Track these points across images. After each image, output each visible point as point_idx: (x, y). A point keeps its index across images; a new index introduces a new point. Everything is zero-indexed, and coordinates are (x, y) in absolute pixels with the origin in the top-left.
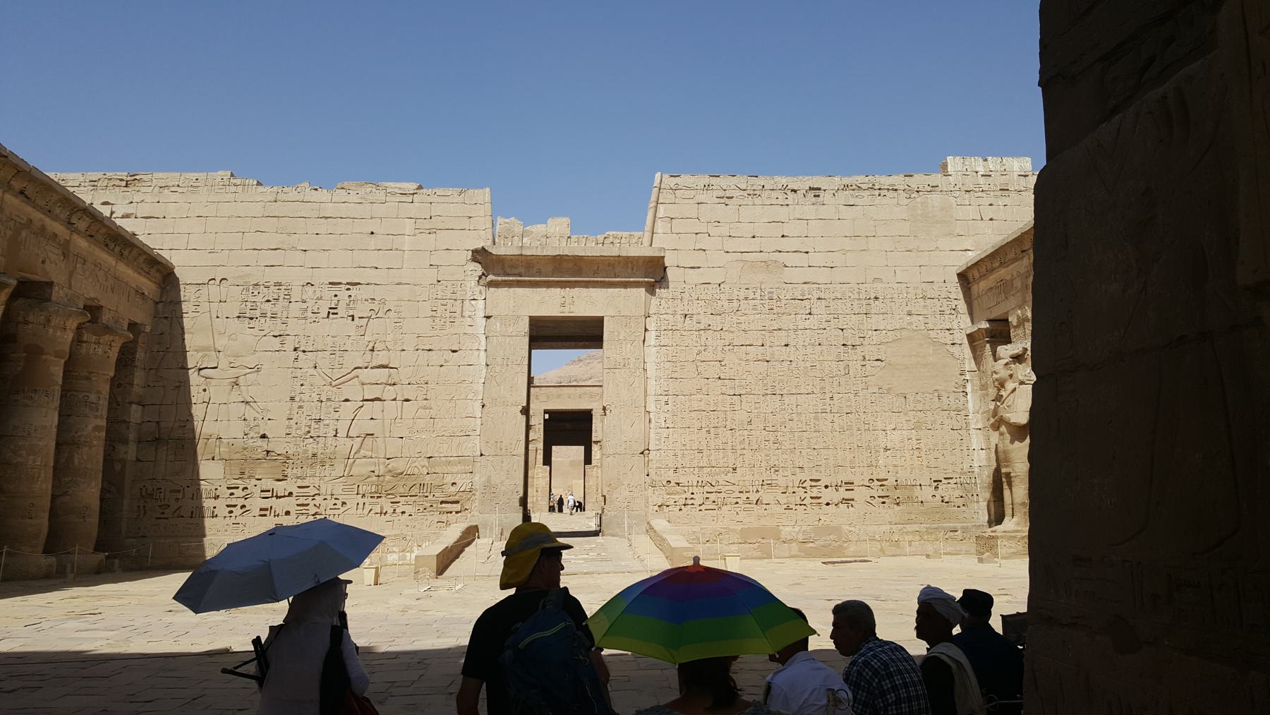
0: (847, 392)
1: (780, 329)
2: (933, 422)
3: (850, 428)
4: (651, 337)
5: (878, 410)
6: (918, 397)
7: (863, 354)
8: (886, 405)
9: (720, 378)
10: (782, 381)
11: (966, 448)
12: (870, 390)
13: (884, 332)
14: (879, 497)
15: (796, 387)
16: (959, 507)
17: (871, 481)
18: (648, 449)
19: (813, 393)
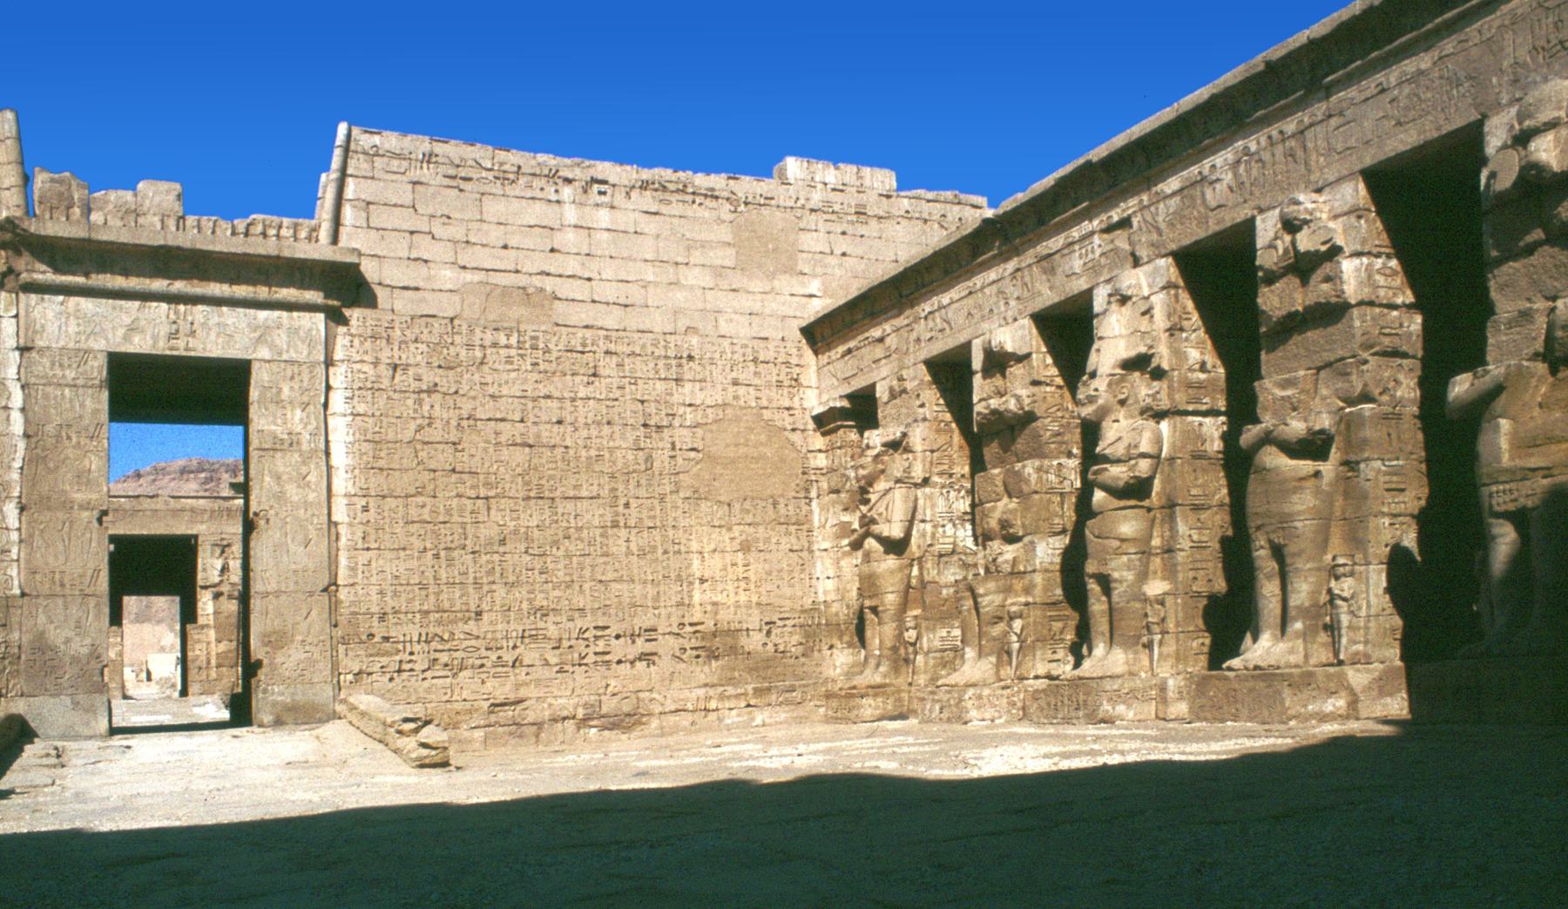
2: (767, 541)
4: (338, 401)
6: (747, 505)
9: (453, 470)
12: (682, 495)
18: (335, 584)
19: (598, 497)
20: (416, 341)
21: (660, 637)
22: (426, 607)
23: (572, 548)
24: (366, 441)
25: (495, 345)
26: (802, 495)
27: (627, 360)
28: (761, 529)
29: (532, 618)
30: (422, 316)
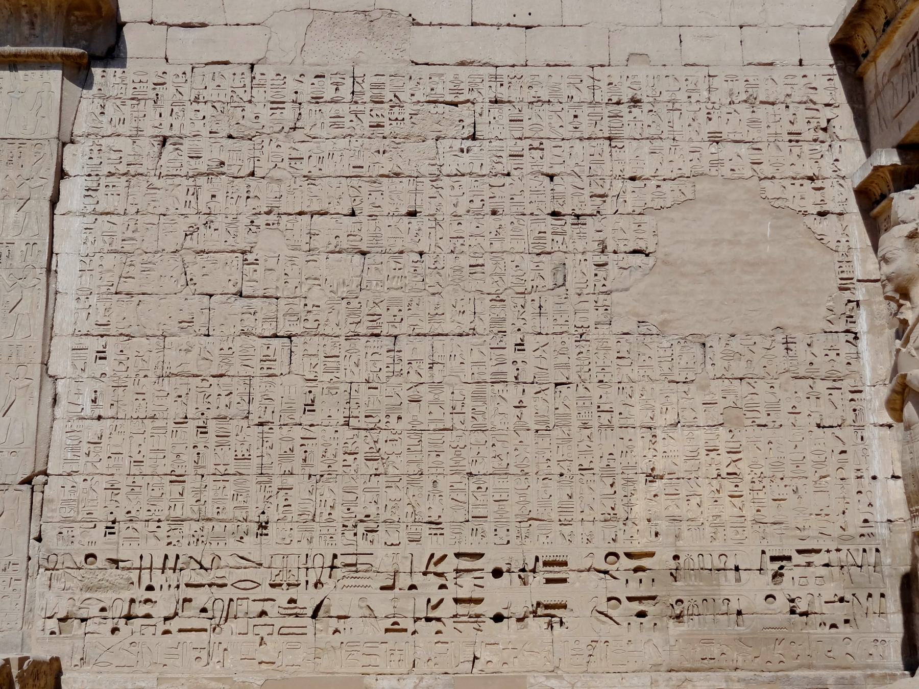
0: (558, 329)
1: (397, 175)
3: (563, 422)
4: (72, 192)
5: (634, 376)
6: (735, 344)
7: (601, 236)
8: (654, 362)
10: (396, 301)
11: (853, 475)
12: (617, 327)
13: (654, 182)
14: (630, 599)
15: (432, 317)
16: (833, 626)
17: (611, 558)
18: (45, 473)
19: (474, 332)
20: (197, 100)
21: (572, 576)
22: (178, 513)
23: (423, 417)
24: (110, 252)
25: (317, 100)
26: (842, 326)
27: (527, 112)
28: (762, 387)
29: (349, 535)
30: (206, 64)
